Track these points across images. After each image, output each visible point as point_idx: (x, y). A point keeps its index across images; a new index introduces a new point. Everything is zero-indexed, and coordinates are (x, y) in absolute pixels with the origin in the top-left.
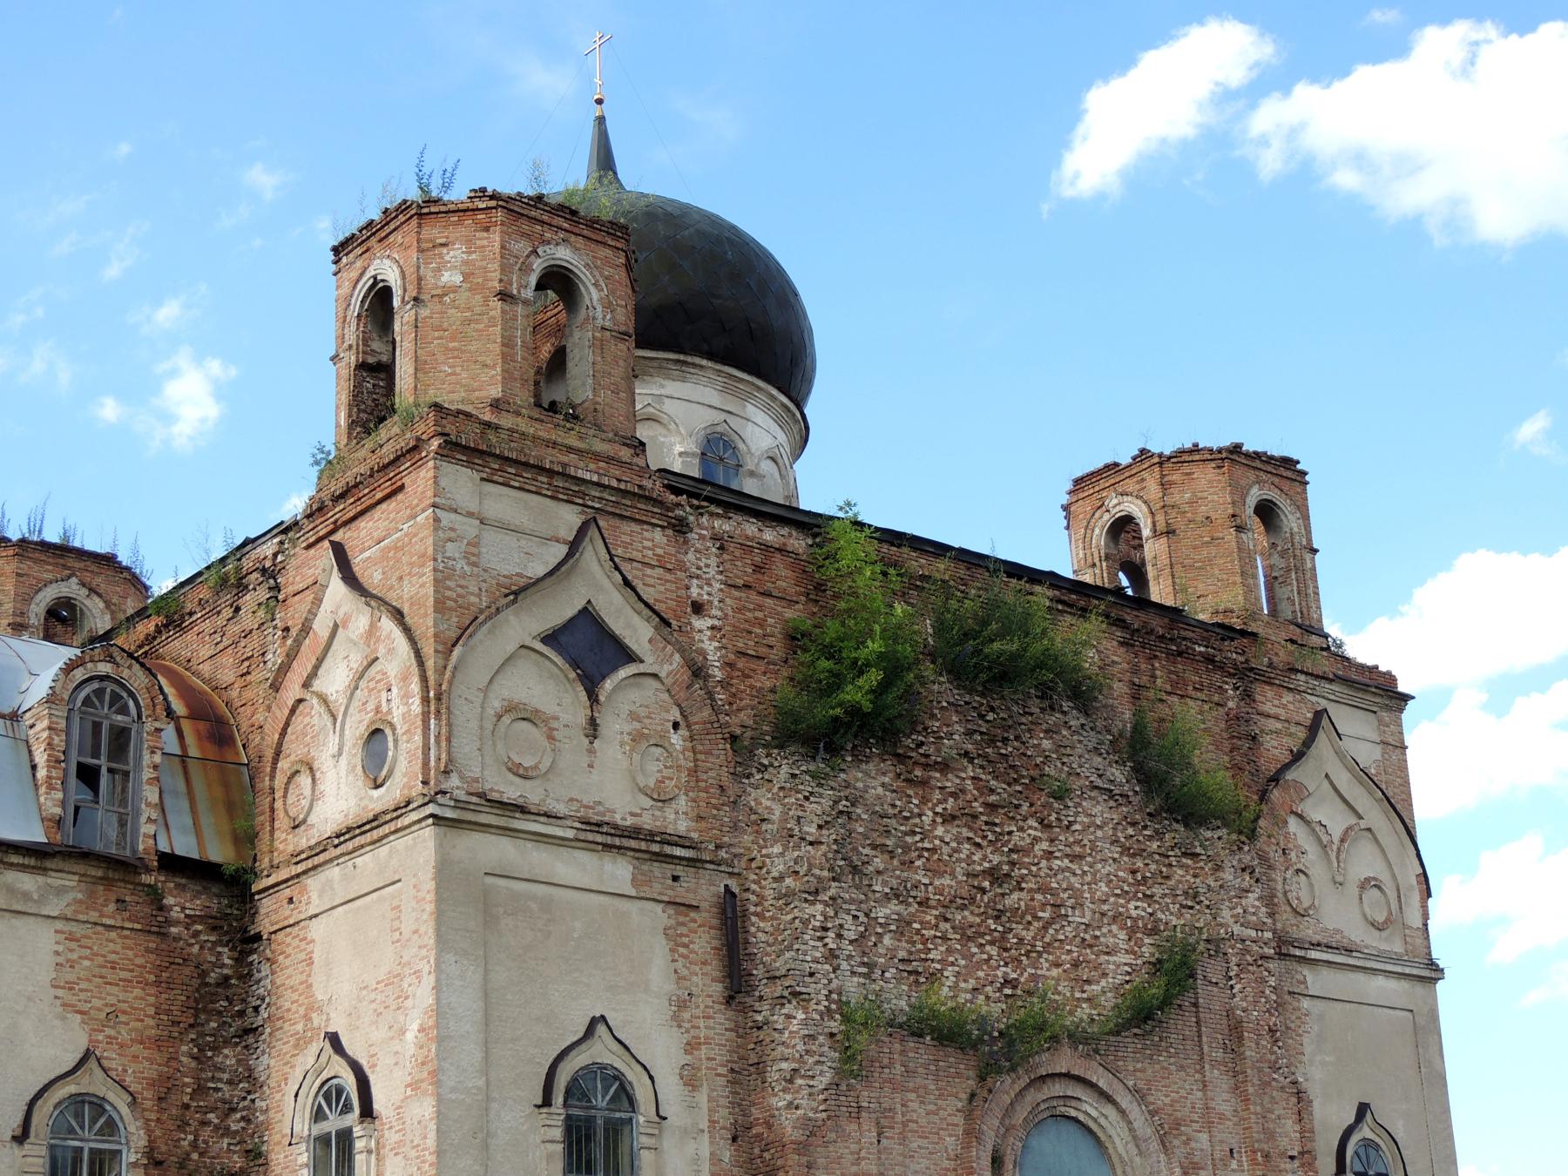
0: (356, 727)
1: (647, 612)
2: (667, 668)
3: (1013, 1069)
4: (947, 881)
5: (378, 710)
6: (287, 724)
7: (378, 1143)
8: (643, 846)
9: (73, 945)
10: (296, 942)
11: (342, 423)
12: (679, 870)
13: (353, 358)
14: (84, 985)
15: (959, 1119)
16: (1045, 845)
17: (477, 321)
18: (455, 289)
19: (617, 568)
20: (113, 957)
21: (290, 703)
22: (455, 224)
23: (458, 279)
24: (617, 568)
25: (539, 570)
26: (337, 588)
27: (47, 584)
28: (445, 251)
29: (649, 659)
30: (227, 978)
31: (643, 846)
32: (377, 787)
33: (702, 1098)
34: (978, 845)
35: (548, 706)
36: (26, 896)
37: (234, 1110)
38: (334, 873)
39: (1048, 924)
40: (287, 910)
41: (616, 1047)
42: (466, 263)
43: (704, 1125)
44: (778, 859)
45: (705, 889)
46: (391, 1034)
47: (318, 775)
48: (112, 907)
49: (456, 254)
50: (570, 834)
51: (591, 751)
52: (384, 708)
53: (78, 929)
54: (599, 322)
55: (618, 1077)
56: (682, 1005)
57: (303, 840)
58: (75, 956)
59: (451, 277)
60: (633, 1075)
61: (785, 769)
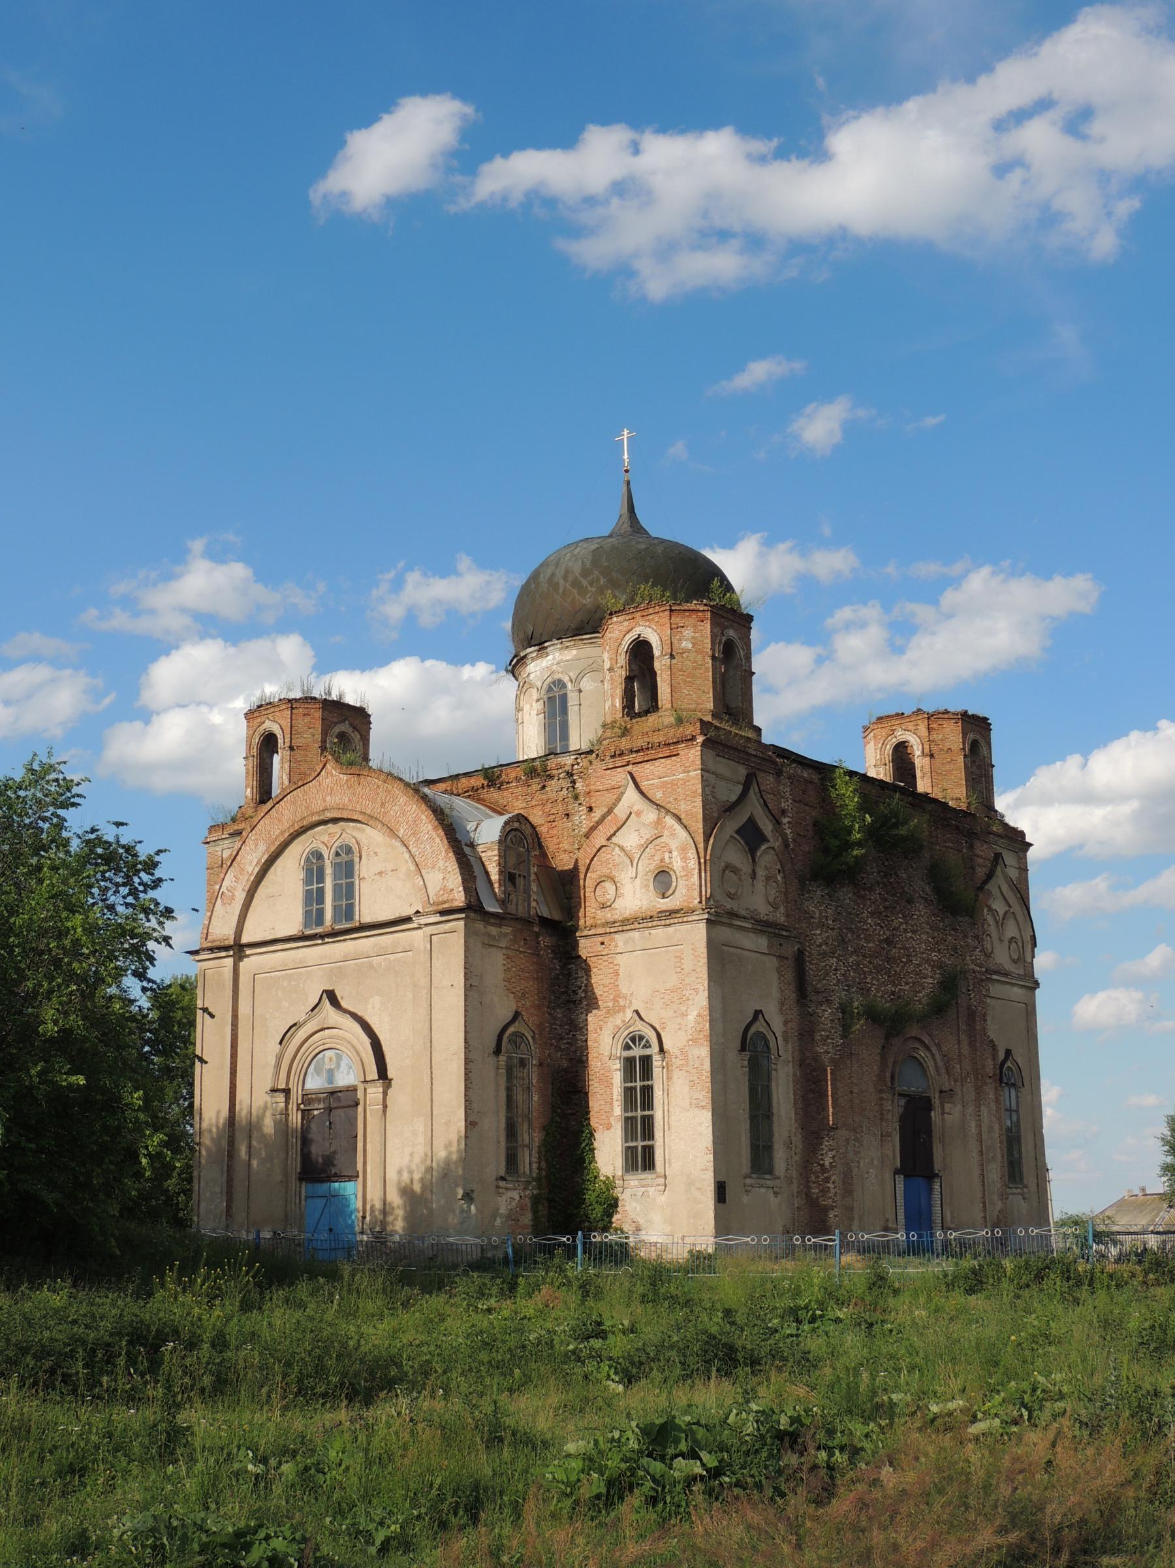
0: (647, 866)
1: (771, 818)
2: (777, 844)
3: (897, 1035)
4: (871, 945)
5: (662, 860)
6: (595, 856)
7: (667, 1063)
8: (773, 930)
9: (509, 961)
10: (607, 963)
11: (617, 705)
12: (782, 941)
13: (624, 673)
14: (513, 980)
15: (878, 1058)
16: (904, 926)
17: (700, 669)
18: (689, 651)
19: (762, 797)
20: (522, 966)
21: (598, 846)
22: (688, 616)
23: (690, 646)
24: (762, 797)
25: (733, 798)
26: (631, 794)
27: (336, 724)
28: (683, 630)
29: (771, 840)
30: (558, 975)
31: (773, 930)
32: (664, 898)
33: (790, 1047)
34: (881, 927)
35: (739, 866)
36: (494, 938)
37: (562, 1039)
38: (636, 935)
39: (906, 963)
40: (600, 948)
41: (765, 1024)
42: (693, 638)
43: (790, 1059)
44: (819, 936)
45: (791, 949)
46: (675, 1015)
47: (618, 885)
48: (522, 942)
49: (688, 632)
50: (750, 926)
51: (753, 885)
52: (667, 860)
53: (510, 953)
54: (744, 668)
55: (765, 1037)
56: (782, 1004)
57: (608, 915)
58: (510, 966)
59: (687, 645)
60: (770, 1037)
61: (819, 893)
